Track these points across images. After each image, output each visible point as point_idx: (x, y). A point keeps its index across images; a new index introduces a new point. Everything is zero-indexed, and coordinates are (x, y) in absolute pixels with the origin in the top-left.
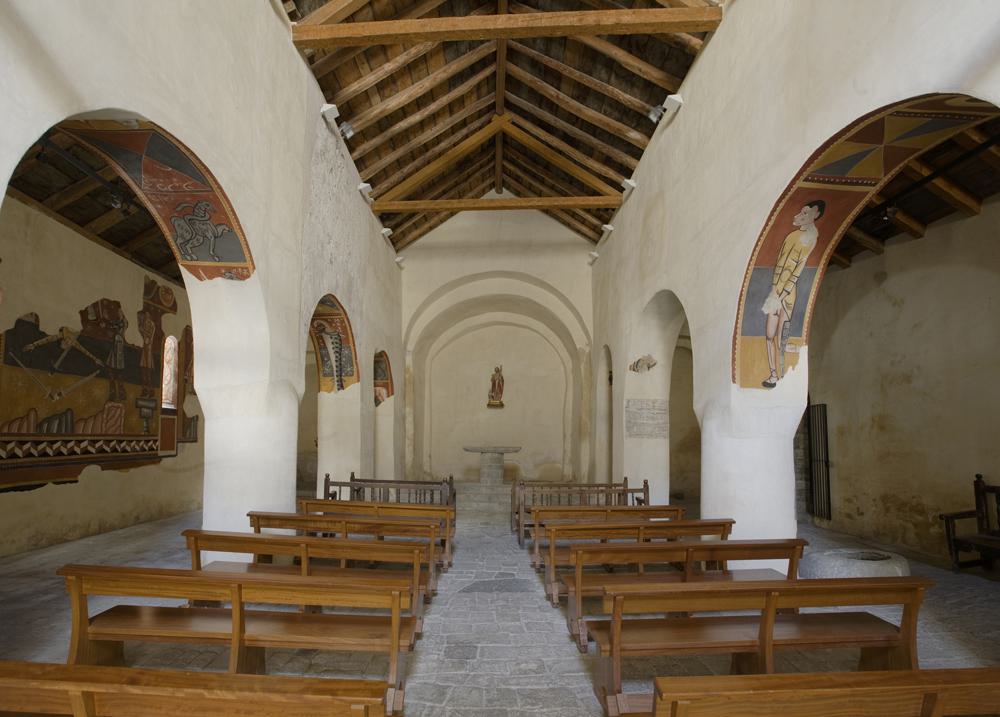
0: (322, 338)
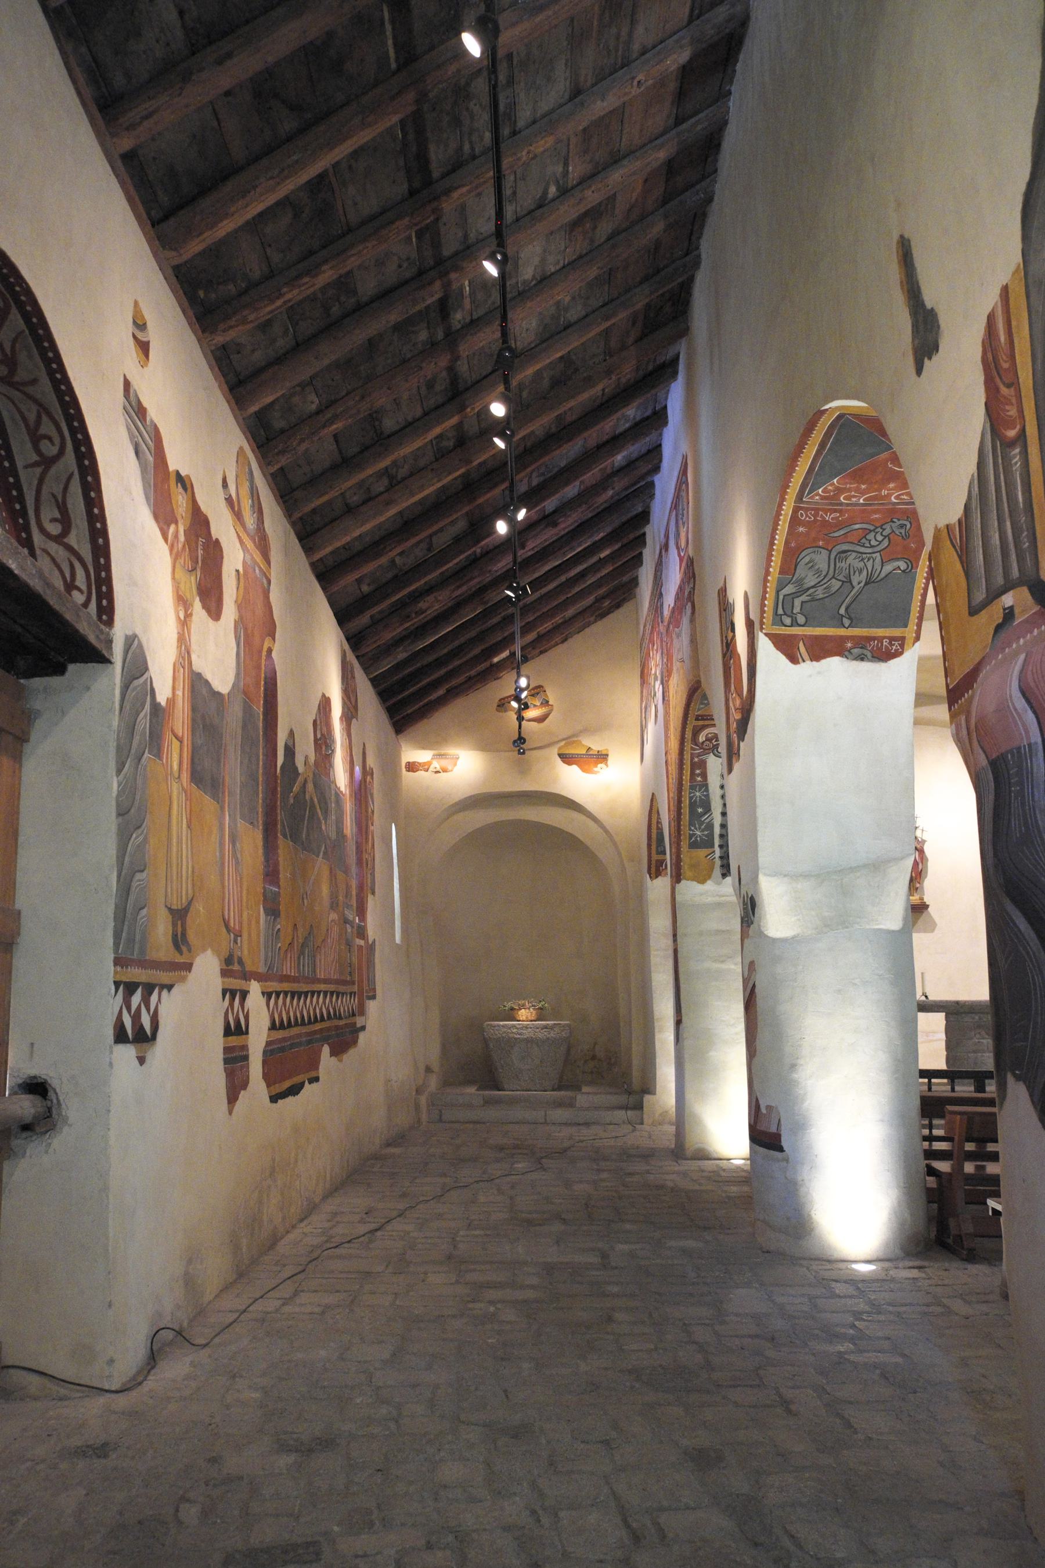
0: (703, 765)
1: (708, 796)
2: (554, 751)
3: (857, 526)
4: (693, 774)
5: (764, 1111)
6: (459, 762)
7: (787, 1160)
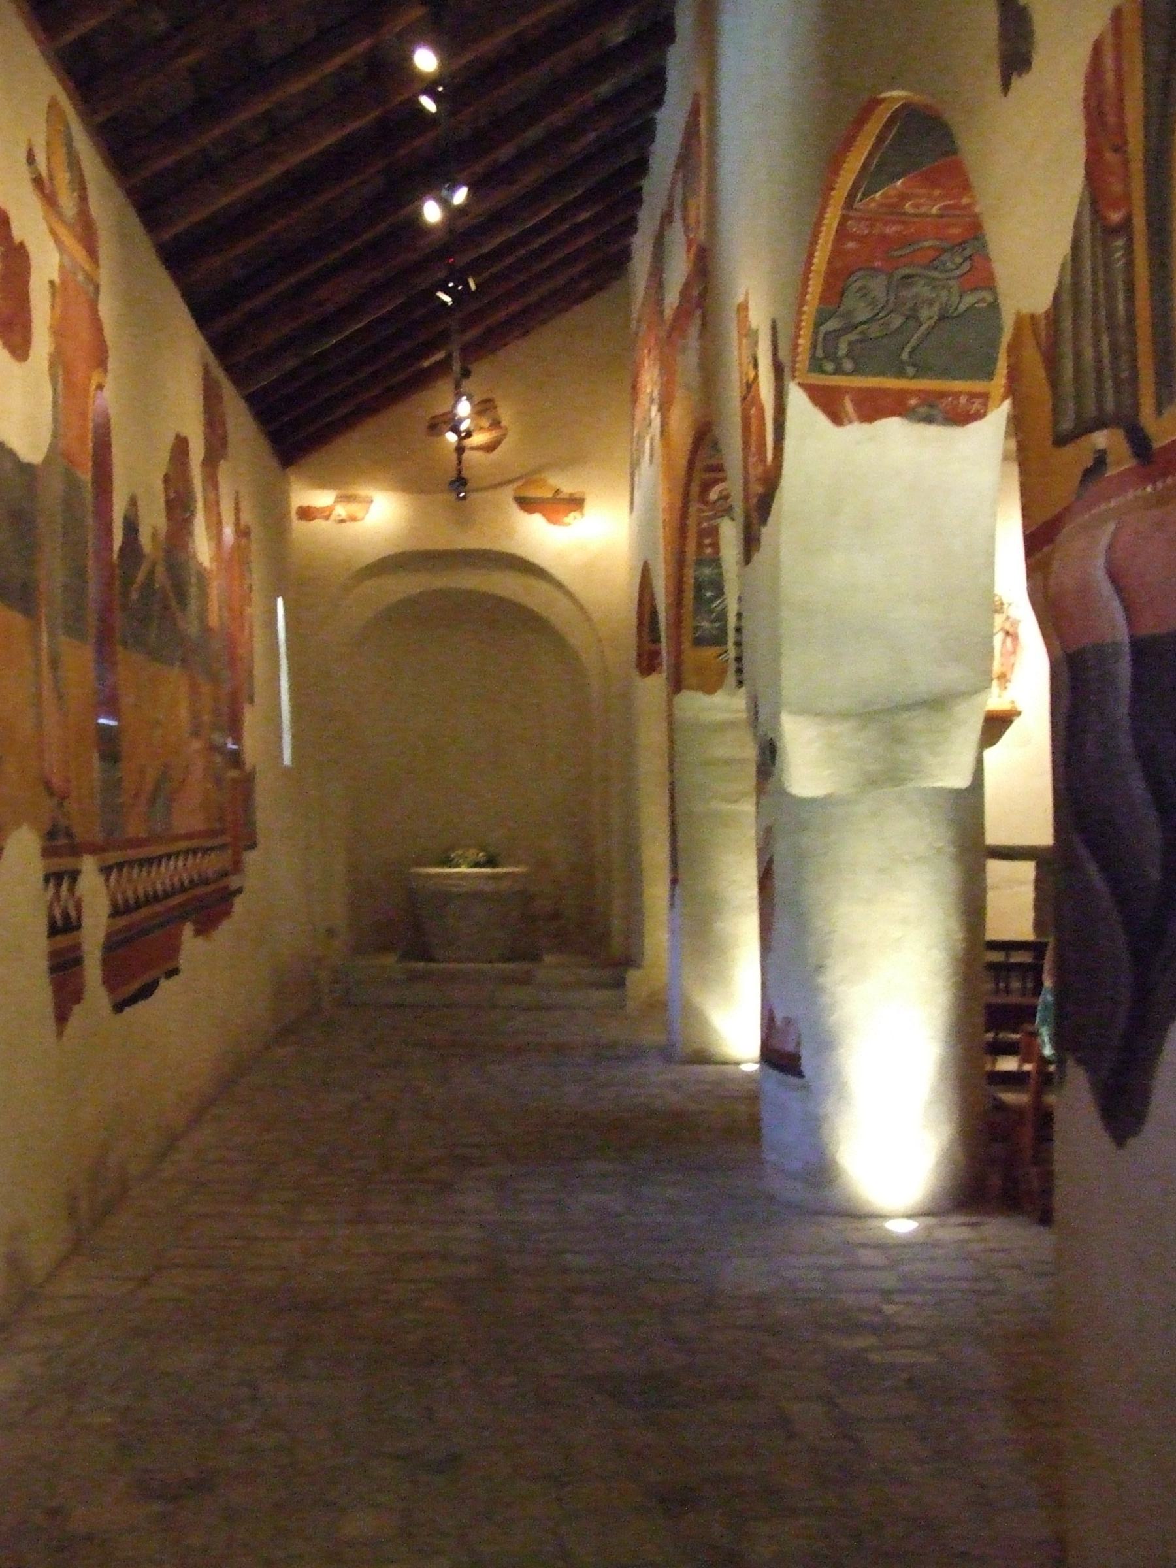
0: (714, 532)
1: (721, 574)
2: (507, 495)
3: (927, 244)
4: (700, 546)
5: (779, 1023)
6: (373, 507)
7: (806, 1088)
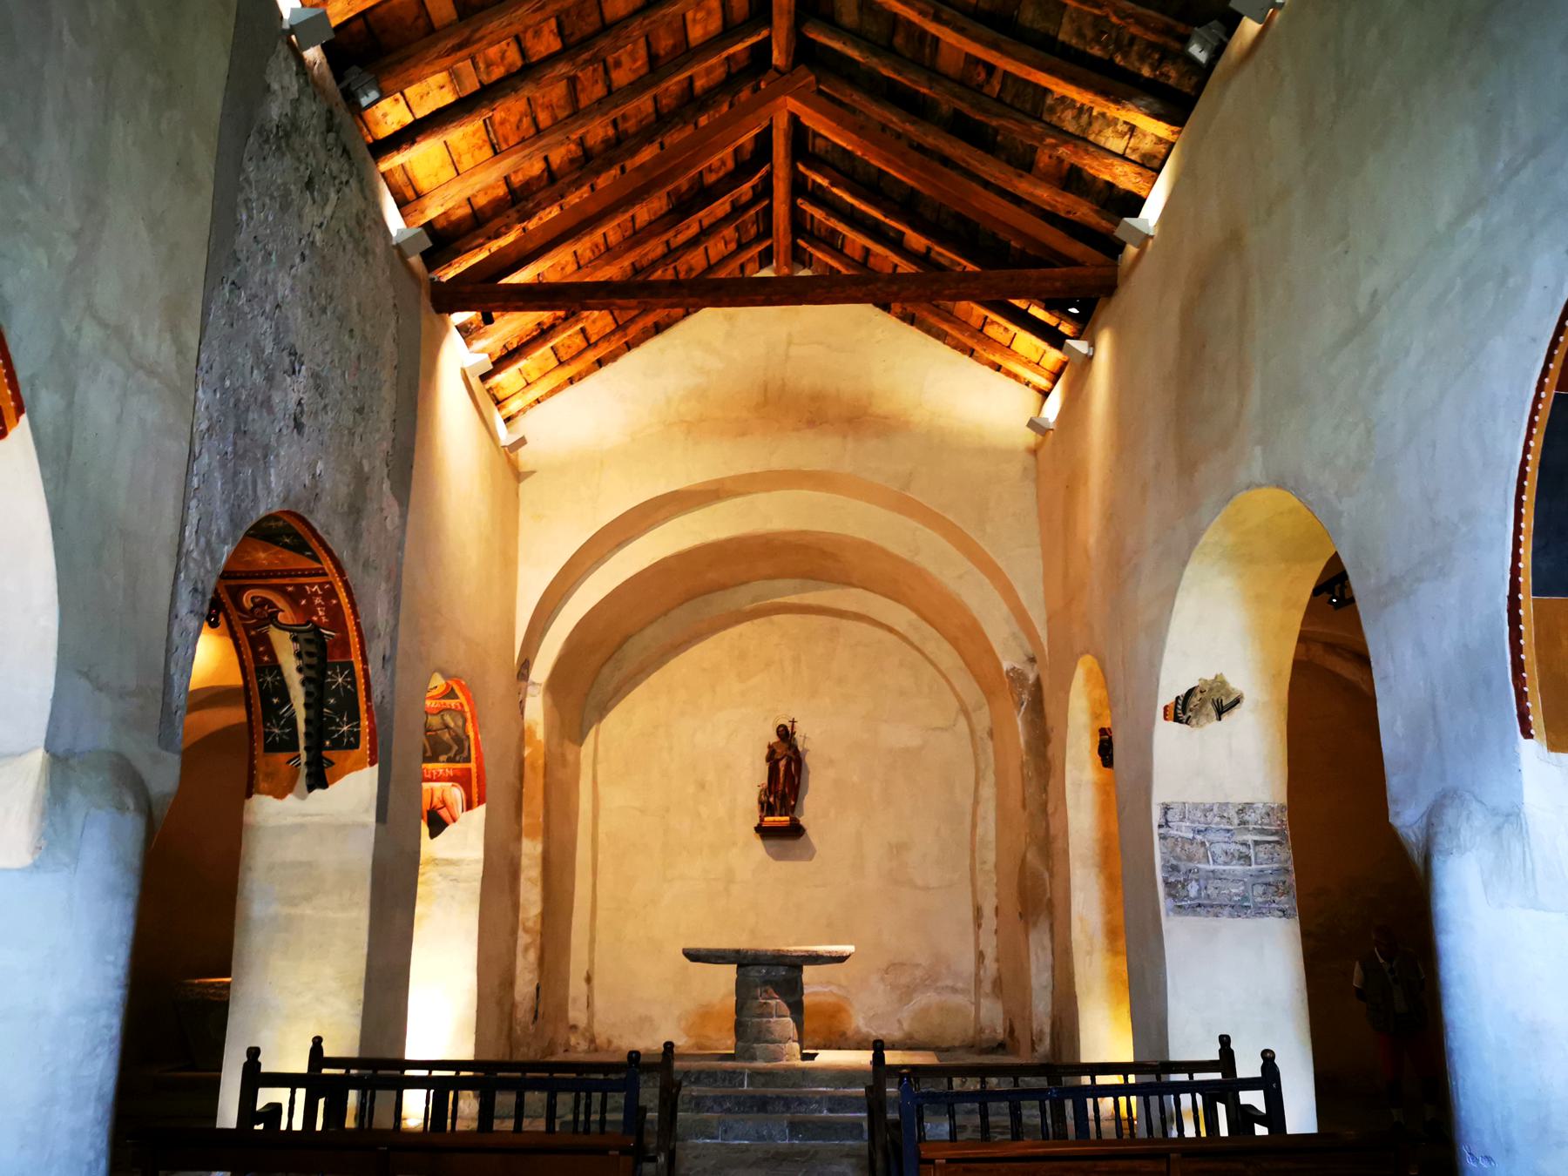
0: (266, 640)
